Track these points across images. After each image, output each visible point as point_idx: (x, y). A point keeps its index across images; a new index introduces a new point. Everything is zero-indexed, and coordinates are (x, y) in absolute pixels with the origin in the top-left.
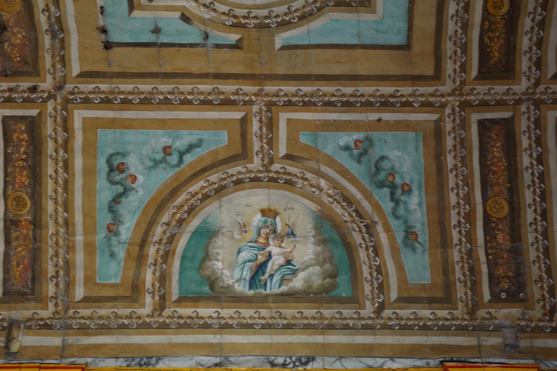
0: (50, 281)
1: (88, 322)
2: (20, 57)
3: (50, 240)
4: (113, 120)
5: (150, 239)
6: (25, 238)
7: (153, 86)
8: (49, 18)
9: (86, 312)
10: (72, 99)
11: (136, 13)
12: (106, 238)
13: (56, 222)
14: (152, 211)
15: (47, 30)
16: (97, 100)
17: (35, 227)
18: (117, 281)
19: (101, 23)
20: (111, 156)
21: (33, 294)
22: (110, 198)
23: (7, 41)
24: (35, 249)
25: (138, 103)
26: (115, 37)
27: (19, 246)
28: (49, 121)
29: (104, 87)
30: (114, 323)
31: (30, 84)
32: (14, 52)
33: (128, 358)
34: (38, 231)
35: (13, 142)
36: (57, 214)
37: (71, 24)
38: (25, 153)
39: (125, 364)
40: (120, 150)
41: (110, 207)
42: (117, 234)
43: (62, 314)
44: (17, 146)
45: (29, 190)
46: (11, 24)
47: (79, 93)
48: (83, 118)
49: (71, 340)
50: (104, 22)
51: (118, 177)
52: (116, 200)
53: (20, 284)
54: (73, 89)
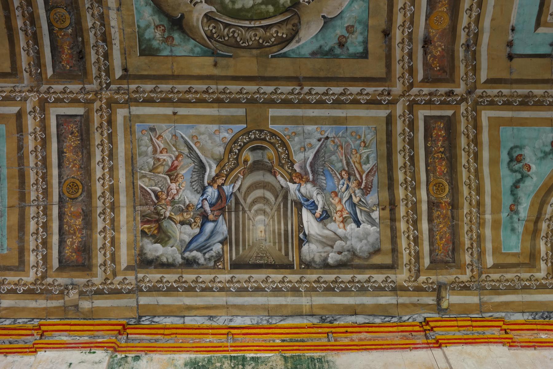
0: (466, 251)
1: (497, 284)
2: (439, 66)
3: (465, 219)
4: (512, 118)
5: (543, 217)
6: (445, 217)
7: (545, 91)
8: (468, 34)
9: (495, 276)
10: (481, 102)
11: (541, 30)
12: (509, 216)
13: (470, 204)
14: (543, 193)
15: (463, 44)
16: (500, 102)
17: (453, 207)
18: (518, 250)
19: (510, 38)
20: (512, 149)
21: (454, 262)
22: (511, 184)
23: (430, 53)
24: (453, 226)
25: (533, 105)
26: (518, 49)
27: (440, 223)
28: (463, 120)
29: (505, 91)
30: (518, 285)
31: (447, 89)
32: (435, 62)
33: (533, 312)
34: (455, 211)
35: (432, 137)
36: (471, 197)
37: (485, 39)
38: (442, 146)
39: (530, 318)
40: (519, 144)
41: (512, 191)
42: (517, 212)
43: (477, 278)
44: (436, 141)
45: (447, 178)
46: (435, 39)
47: (487, 96)
48: (488, 117)
49: (485, 298)
50: (512, 37)
51: (517, 166)
52: (516, 186)
53: (443, 254)
54: (482, 93)
